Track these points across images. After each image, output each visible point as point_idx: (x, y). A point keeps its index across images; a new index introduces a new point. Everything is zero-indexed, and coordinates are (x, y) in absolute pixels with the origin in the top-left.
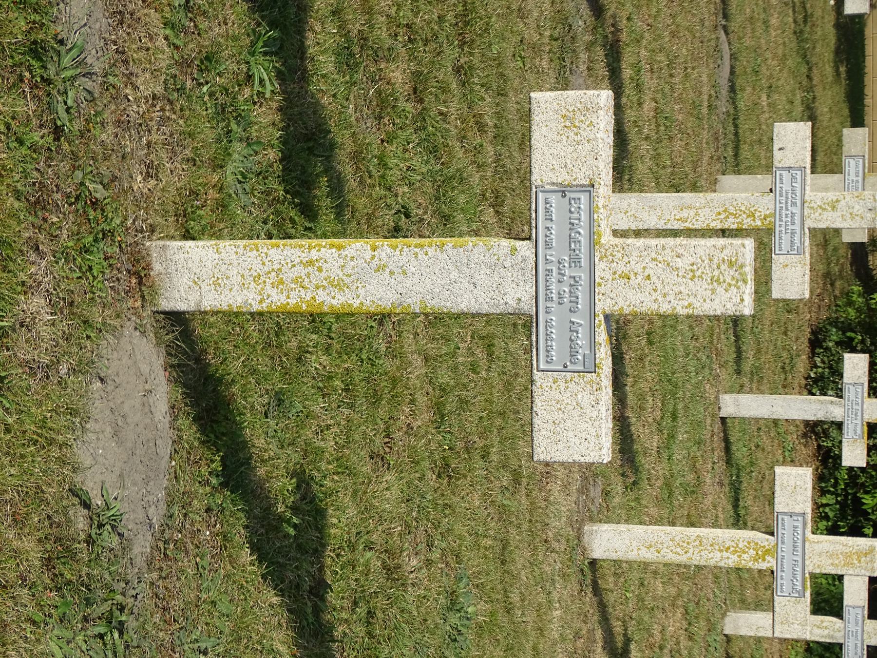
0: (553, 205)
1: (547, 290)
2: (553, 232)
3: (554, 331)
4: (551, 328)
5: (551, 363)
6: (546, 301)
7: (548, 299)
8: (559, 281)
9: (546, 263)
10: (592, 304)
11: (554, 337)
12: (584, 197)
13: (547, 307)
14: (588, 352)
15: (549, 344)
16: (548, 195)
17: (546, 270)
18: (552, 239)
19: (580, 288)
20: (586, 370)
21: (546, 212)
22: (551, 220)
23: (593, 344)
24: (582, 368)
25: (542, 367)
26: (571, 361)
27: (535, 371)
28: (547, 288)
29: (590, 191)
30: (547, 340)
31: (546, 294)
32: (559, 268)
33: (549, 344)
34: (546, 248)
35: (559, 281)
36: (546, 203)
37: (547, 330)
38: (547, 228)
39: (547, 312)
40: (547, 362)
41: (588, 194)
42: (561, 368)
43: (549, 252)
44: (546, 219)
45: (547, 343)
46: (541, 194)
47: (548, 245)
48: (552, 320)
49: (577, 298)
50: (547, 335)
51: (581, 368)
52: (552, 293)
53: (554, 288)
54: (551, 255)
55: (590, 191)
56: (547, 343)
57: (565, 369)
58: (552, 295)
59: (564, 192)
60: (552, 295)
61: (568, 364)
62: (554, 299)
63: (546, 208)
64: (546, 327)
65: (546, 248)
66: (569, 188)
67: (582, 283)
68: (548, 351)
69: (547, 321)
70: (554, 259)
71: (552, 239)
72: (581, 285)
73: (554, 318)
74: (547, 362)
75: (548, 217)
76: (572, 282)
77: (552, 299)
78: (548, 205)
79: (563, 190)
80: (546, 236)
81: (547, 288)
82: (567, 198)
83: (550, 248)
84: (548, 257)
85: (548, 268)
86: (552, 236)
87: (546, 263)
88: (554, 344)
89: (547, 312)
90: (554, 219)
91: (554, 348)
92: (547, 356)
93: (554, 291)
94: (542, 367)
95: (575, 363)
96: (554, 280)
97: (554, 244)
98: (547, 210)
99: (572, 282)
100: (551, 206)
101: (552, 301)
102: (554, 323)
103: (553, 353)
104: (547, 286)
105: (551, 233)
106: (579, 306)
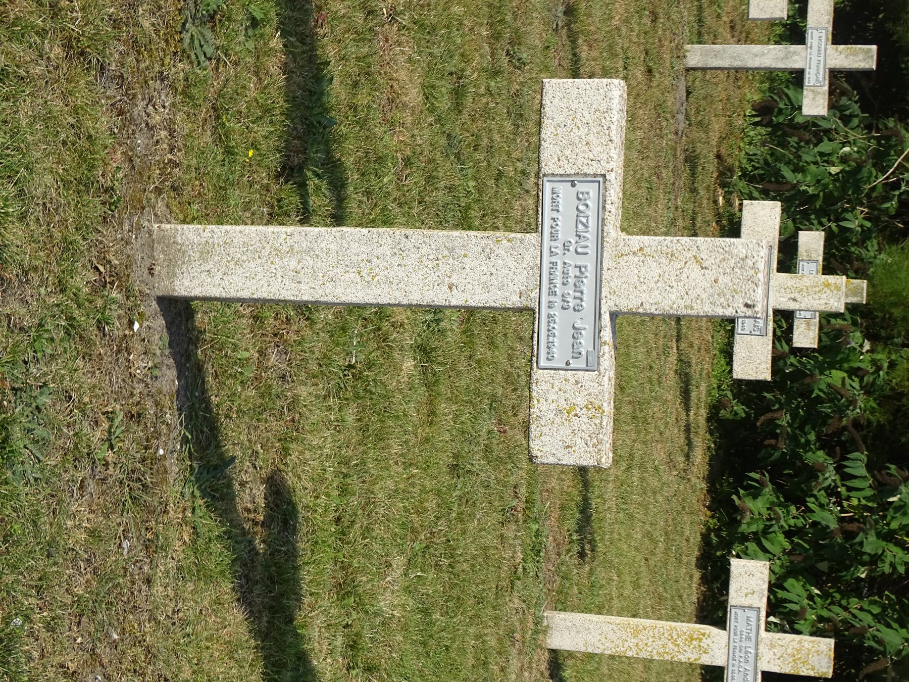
0: (560, 195)
1: (550, 283)
2: (559, 223)
3: (556, 326)
6: (549, 295)
9: (551, 256)
13: (550, 302)
14: (592, 349)
15: (551, 339)
16: (555, 185)
17: (552, 263)
19: (584, 280)
20: (588, 368)
21: (552, 202)
22: (558, 211)
24: (584, 366)
27: (535, 369)
28: (551, 281)
30: (548, 336)
31: (550, 288)
33: (551, 339)
34: (551, 240)
36: (553, 193)
37: (549, 325)
38: (553, 219)
39: (549, 307)
40: (548, 359)
41: (597, 184)
42: (563, 365)
43: (553, 244)
44: (552, 210)
45: (548, 339)
46: (548, 183)
47: (553, 237)
49: (582, 292)
50: (549, 330)
51: (584, 366)
52: (555, 286)
53: (558, 281)
56: (548, 339)
58: (556, 289)
59: (572, 181)
60: (556, 289)
62: (557, 293)
63: (553, 198)
65: (551, 240)
66: (578, 179)
67: (588, 275)
68: (549, 348)
69: (549, 317)
70: (559, 252)
72: (586, 277)
73: (557, 313)
74: (548, 359)
75: (554, 208)
76: (578, 274)
78: (555, 195)
80: (552, 227)
83: (555, 240)
84: (553, 250)
86: (558, 228)
87: (551, 256)
89: (549, 307)
90: (560, 209)
91: (556, 344)
92: (548, 353)
93: (557, 285)
94: (543, 363)
97: (560, 236)
99: (578, 274)
100: (558, 196)
101: (556, 295)
103: (555, 350)
104: (550, 280)
105: (557, 225)
106: (583, 303)
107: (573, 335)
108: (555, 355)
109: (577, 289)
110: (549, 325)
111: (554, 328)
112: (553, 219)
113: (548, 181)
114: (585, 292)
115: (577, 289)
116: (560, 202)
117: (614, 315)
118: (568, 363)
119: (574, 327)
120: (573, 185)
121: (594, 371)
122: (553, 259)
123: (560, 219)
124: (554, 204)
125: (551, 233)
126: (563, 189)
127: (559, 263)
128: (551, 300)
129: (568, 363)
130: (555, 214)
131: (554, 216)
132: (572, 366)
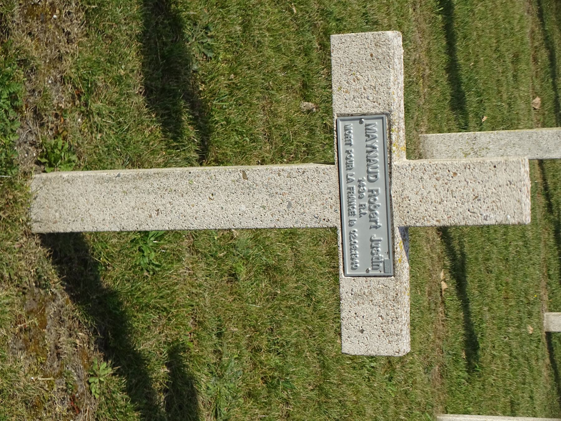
0: (352, 131)
1: (349, 205)
2: (353, 155)
3: (357, 241)
4: (354, 239)
5: (356, 269)
6: (349, 215)
7: (352, 214)
8: (360, 198)
10: (390, 216)
11: (357, 246)
12: (378, 123)
13: (350, 221)
14: (387, 258)
16: (347, 123)
18: (352, 161)
20: (386, 274)
22: (350, 144)
23: (392, 252)
24: (382, 273)
25: (348, 273)
26: (373, 269)
28: (350, 204)
29: (382, 118)
30: (351, 249)
31: (349, 210)
32: (359, 186)
33: (354, 252)
35: (360, 198)
36: (345, 130)
37: (351, 241)
38: (347, 152)
39: (350, 225)
40: (352, 269)
42: (364, 273)
43: (349, 172)
44: (346, 144)
45: (351, 252)
47: (349, 167)
48: (355, 231)
50: (351, 245)
52: (353, 208)
53: (356, 204)
54: (352, 175)
55: (382, 118)
56: (351, 252)
57: (368, 274)
61: (370, 269)
62: (356, 213)
63: (345, 134)
64: (350, 238)
65: (347, 170)
66: (366, 117)
68: (352, 259)
69: (350, 233)
70: (354, 179)
71: (352, 161)
73: (356, 230)
75: (347, 142)
77: (353, 214)
79: (359, 118)
80: (347, 159)
81: (350, 204)
82: (364, 124)
83: (351, 169)
84: (349, 177)
85: (349, 186)
87: (348, 183)
88: (357, 252)
89: (350, 225)
90: (353, 143)
91: (358, 256)
92: (352, 264)
93: (355, 206)
94: (348, 273)
95: (376, 269)
96: (355, 197)
98: (346, 136)
100: (350, 132)
101: (354, 215)
102: (357, 235)
103: (357, 261)
104: (349, 202)
105: (351, 156)
107: (371, 245)
108: (358, 265)
109: (371, 219)
110: (351, 241)
111: (355, 242)
112: (347, 152)
113: (342, 120)
114: (378, 221)
115: (371, 219)
116: (352, 137)
117: (405, 231)
118: (368, 271)
119: (372, 241)
120: (361, 122)
121: (391, 276)
122: (350, 185)
123: (353, 151)
124: (347, 139)
125: (347, 163)
126: (352, 125)
127: (355, 188)
128: (351, 219)
129: (368, 271)
130: (348, 148)
131: (347, 149)
132: (372, 273)
